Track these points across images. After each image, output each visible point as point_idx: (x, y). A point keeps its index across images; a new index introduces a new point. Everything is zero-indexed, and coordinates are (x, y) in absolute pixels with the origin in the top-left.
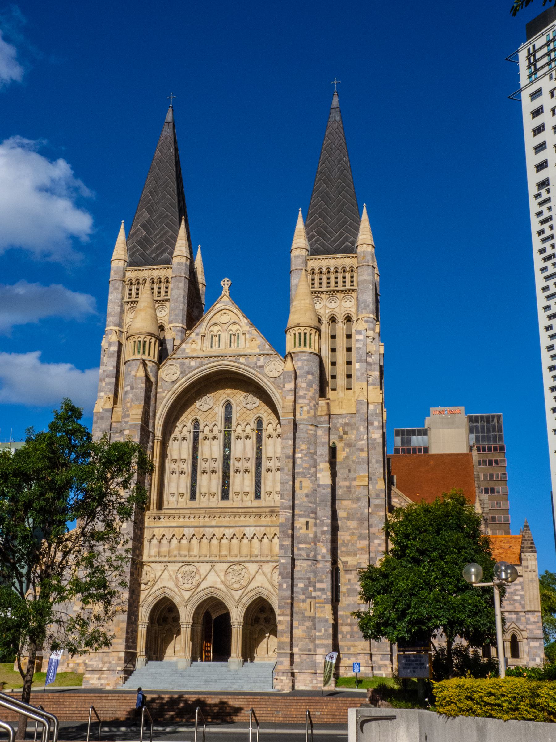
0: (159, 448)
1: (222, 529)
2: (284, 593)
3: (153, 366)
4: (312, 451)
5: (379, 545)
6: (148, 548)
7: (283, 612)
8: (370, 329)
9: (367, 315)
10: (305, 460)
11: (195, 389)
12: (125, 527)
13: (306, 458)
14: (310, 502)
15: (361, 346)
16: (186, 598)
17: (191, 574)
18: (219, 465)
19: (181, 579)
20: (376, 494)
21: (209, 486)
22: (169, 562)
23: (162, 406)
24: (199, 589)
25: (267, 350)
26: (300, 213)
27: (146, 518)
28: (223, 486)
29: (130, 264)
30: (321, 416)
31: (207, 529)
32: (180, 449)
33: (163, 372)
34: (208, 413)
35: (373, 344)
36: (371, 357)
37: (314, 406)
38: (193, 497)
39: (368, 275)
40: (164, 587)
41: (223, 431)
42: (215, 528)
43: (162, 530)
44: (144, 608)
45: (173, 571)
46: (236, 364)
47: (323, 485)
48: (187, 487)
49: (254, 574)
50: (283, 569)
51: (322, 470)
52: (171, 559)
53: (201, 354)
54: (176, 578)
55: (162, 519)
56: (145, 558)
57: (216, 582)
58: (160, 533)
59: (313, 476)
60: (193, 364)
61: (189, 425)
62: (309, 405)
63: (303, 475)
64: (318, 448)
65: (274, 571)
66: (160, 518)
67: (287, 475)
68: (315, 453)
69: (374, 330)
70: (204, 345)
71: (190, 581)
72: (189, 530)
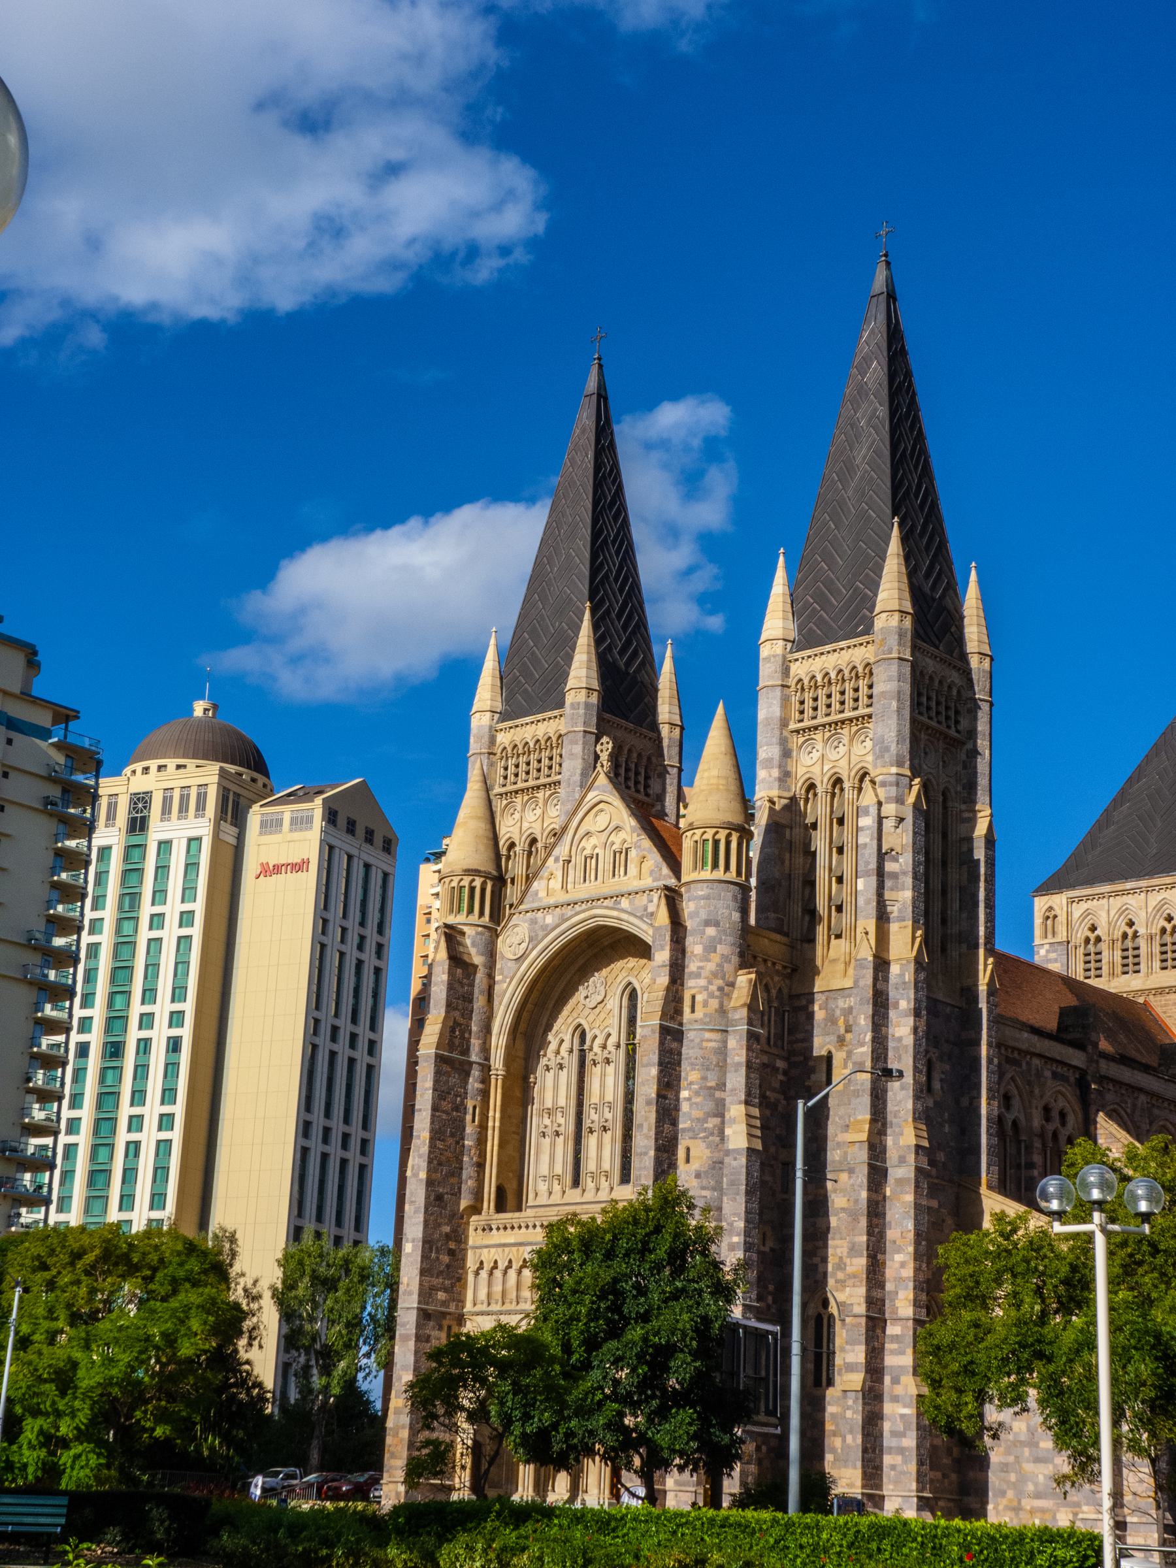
0: (499, 1090)
3: (478, 933)
4: (712, 1084)
5: (903, 1265)
8: (889, 800)
9: (885, 770)
10: (695, 1103)
11: (577, 966)
13: (698, 1100)
14: (703, 1188)
15: (868, 840)
18: (615, 1117)
20: (900, 1157)
21: (599, 1159)
23: (502, 1008)
25: (666, 877)
26: (781, 558)
27: (471, 1229)
29: (505, 716)
30: (735, 1009)
32: (556, 1088)
33: (504, 942)
34: (597, 1011)
35: (899, 830)
36: (897, 861)
37: (720, 989)
38: (576, 1182)
39: (890, 679)
41: (623, 1046)
46: (615, 913)
47: (734, 1150)
51: (734, 1121)
52: (506, 1307)
53: (562, 898)
55: (494, 1231)
56: (469, 1307)
59: (712, 1134)
60: (549, 920)
61: (567, 1038)
62: (706, 989)
63: (691, 1134)
64: (728, 1075)
66: (491, 1229)
67: (647, 1137)
68: (721, 1086)
69: (900, 800)
70: (570, 879)
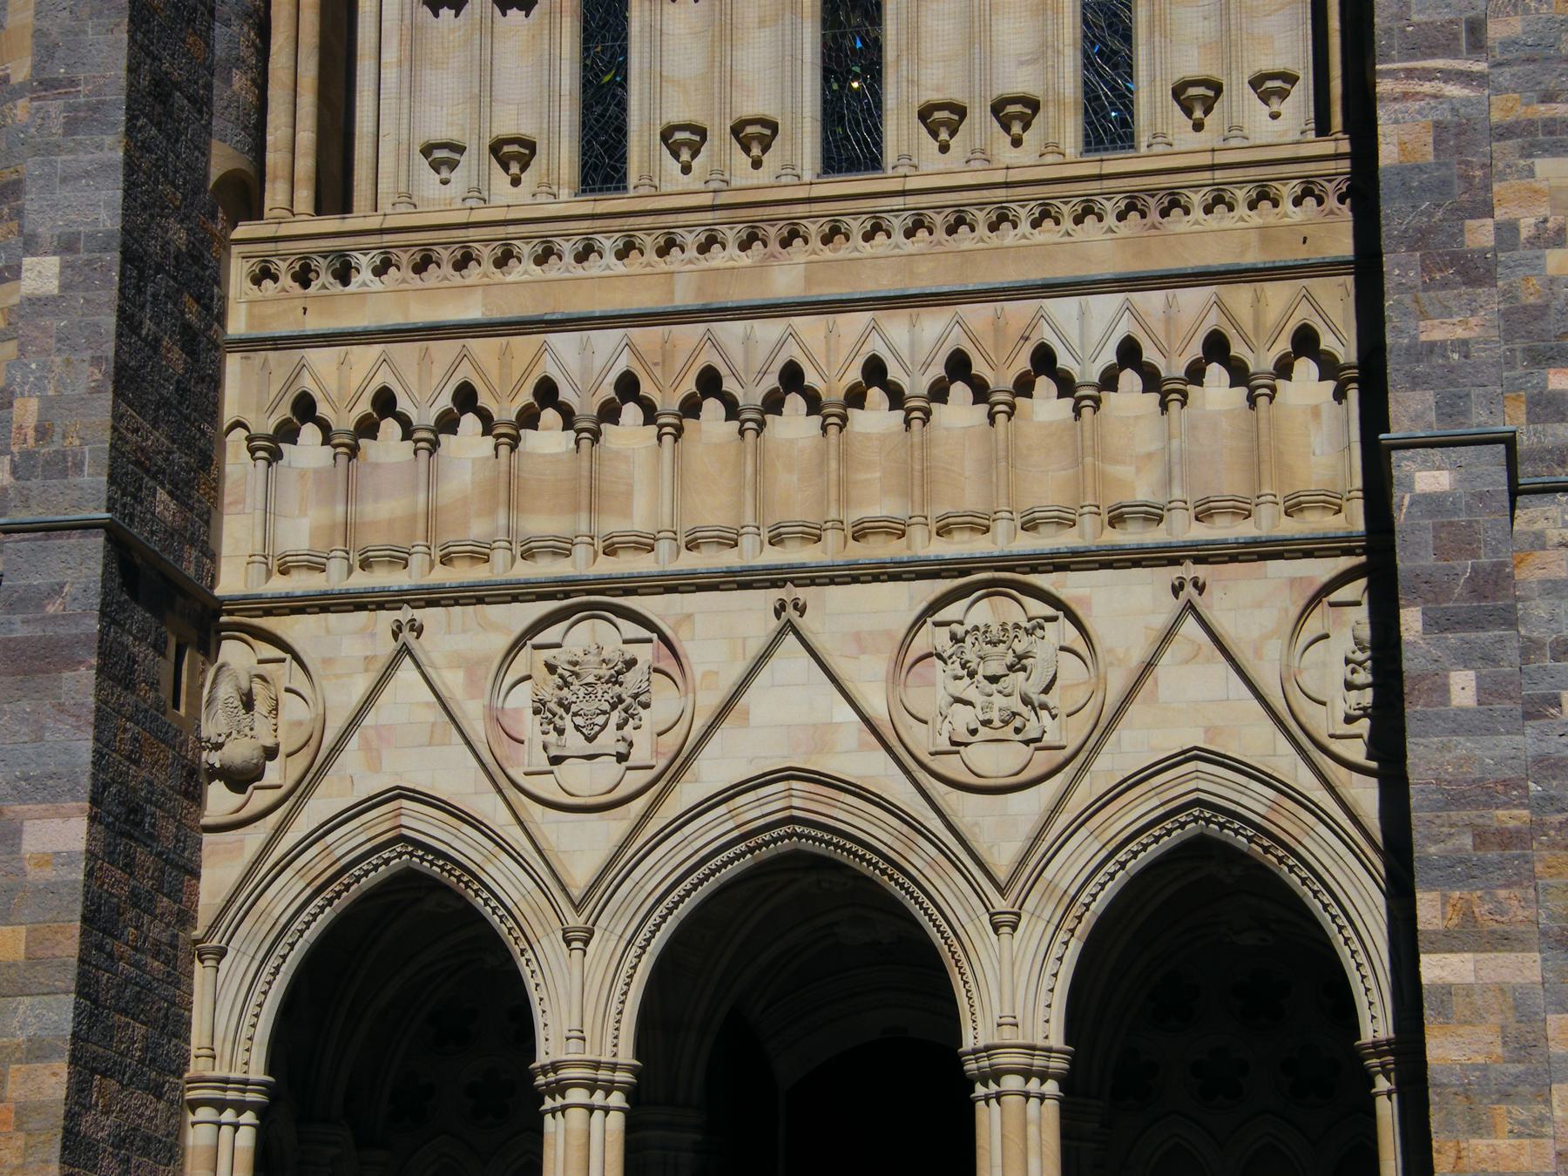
1: (856, 322)
2: (1464, 746)
6: (255, 498)
7: (1469, 917)
12: (52, 287)
16: (580, 875)
17: (615, 680)
19: (530, 727)
22: (433, 598)
24: (686, 795)
27: (238, 271)
28: (827, 74)
31: (731, 332)
40: (401, 793)
42: (797, 321)
43: (365, 356)
44: (237, 965)
45: (470, 666)
48: (551, 93)
49: (1138, 656)
50: (1439, 552)
54: (496, 718)
55: (363, 277)
57: (822, 733)
58: (356, 380)
65: (1313, 625)
66: (344, 274)
71: (608, 740)
72: (584, 348)
